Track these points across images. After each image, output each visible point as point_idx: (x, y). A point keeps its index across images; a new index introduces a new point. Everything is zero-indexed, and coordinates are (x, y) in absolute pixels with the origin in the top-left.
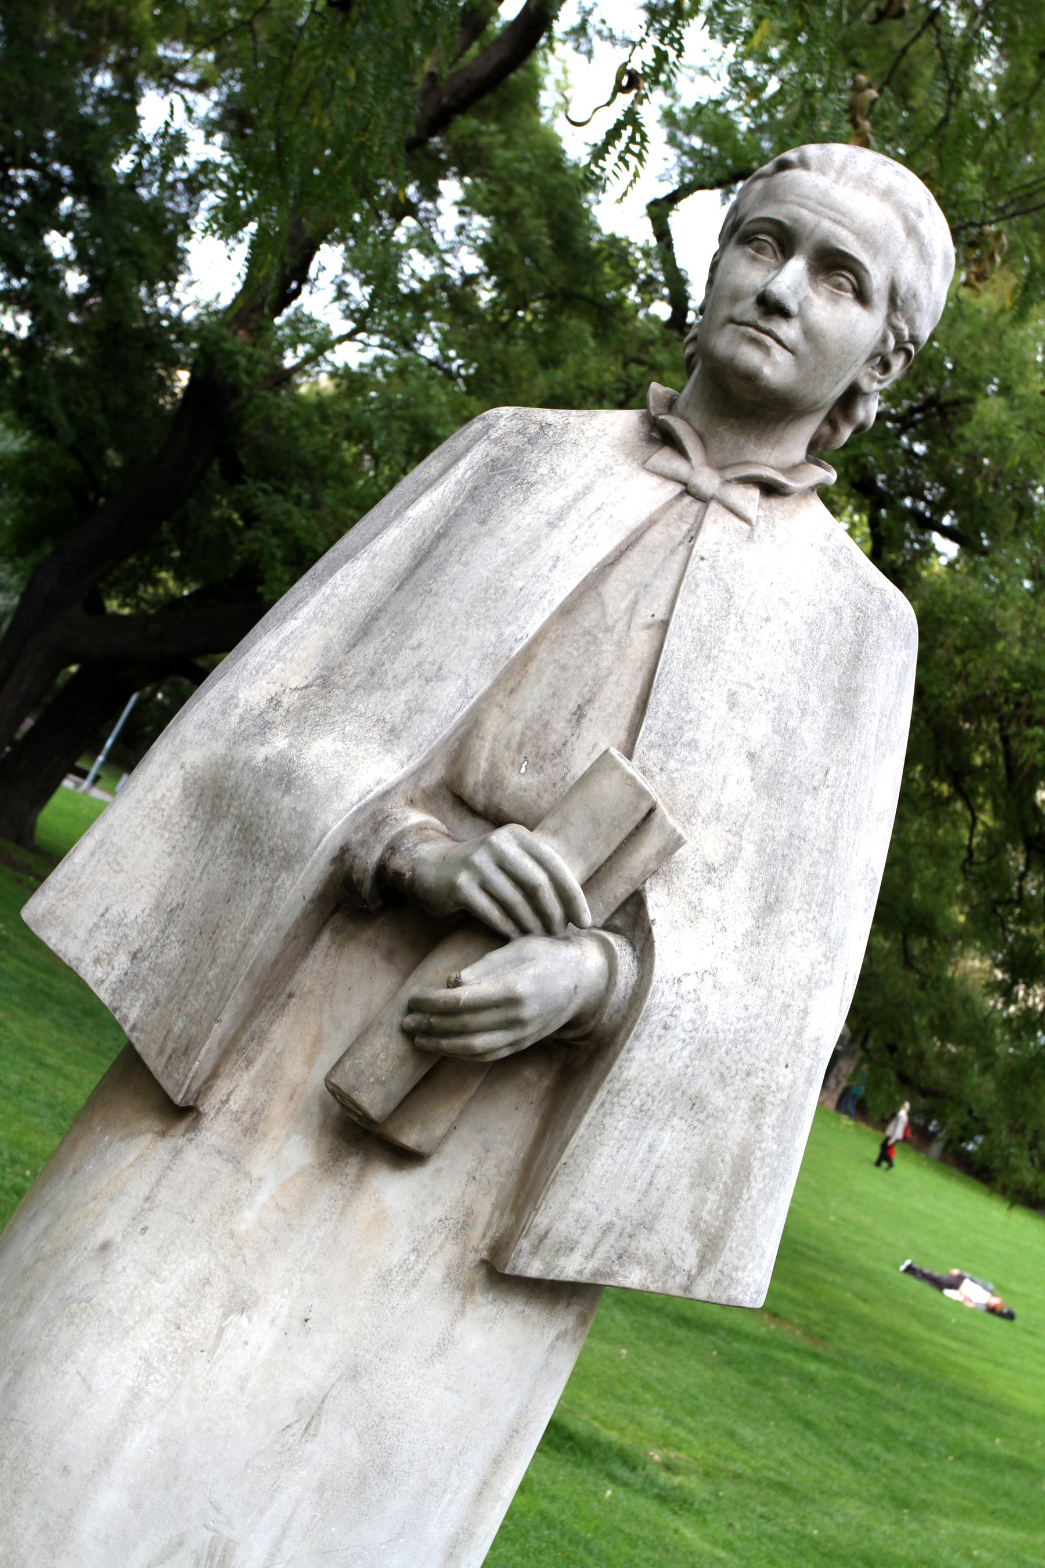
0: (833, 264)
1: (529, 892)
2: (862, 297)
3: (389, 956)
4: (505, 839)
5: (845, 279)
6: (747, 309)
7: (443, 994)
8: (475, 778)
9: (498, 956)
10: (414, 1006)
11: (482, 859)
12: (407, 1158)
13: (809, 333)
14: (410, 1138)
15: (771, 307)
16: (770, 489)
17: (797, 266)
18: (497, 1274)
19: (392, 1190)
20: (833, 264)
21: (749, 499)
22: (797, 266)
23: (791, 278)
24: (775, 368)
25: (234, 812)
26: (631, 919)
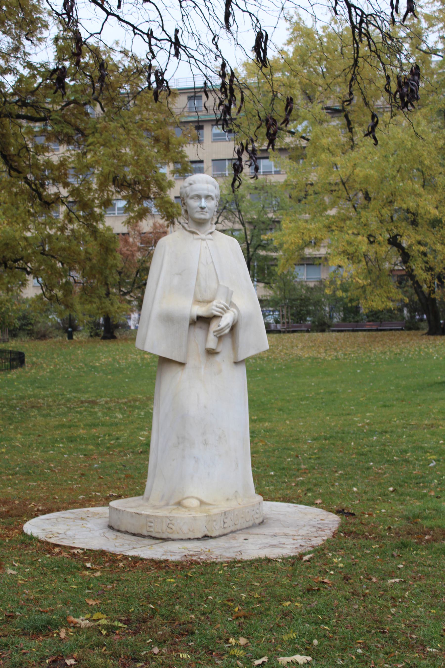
0: (207, 197)
1: (222, 309)
2: (213, 199)
3: (201, 328)
4: (214, 303)
5: (210, 198)
6: (199, 209)
7: (219, 328)
8: (199, 297)
9: (223, 319)
10: (214, 332)
11: (214, 308)
12: (217, 353)
13: (209, 209)
14: (218, 350)
15: (202, 208)
16: (211, 233)
17: (203, 200)
18: (236, 363)
19: (218, 358)
20: (207, 197)
21: (210, 236)
22: (203, 200)
23: (204, 203)
24: (208, 216)
25: (168, 319)
26: (232, 304)
